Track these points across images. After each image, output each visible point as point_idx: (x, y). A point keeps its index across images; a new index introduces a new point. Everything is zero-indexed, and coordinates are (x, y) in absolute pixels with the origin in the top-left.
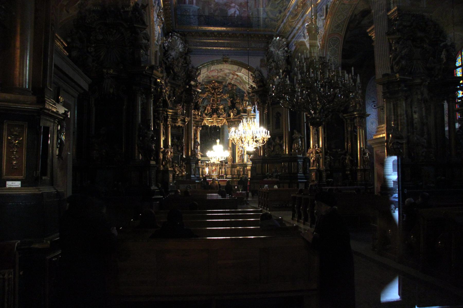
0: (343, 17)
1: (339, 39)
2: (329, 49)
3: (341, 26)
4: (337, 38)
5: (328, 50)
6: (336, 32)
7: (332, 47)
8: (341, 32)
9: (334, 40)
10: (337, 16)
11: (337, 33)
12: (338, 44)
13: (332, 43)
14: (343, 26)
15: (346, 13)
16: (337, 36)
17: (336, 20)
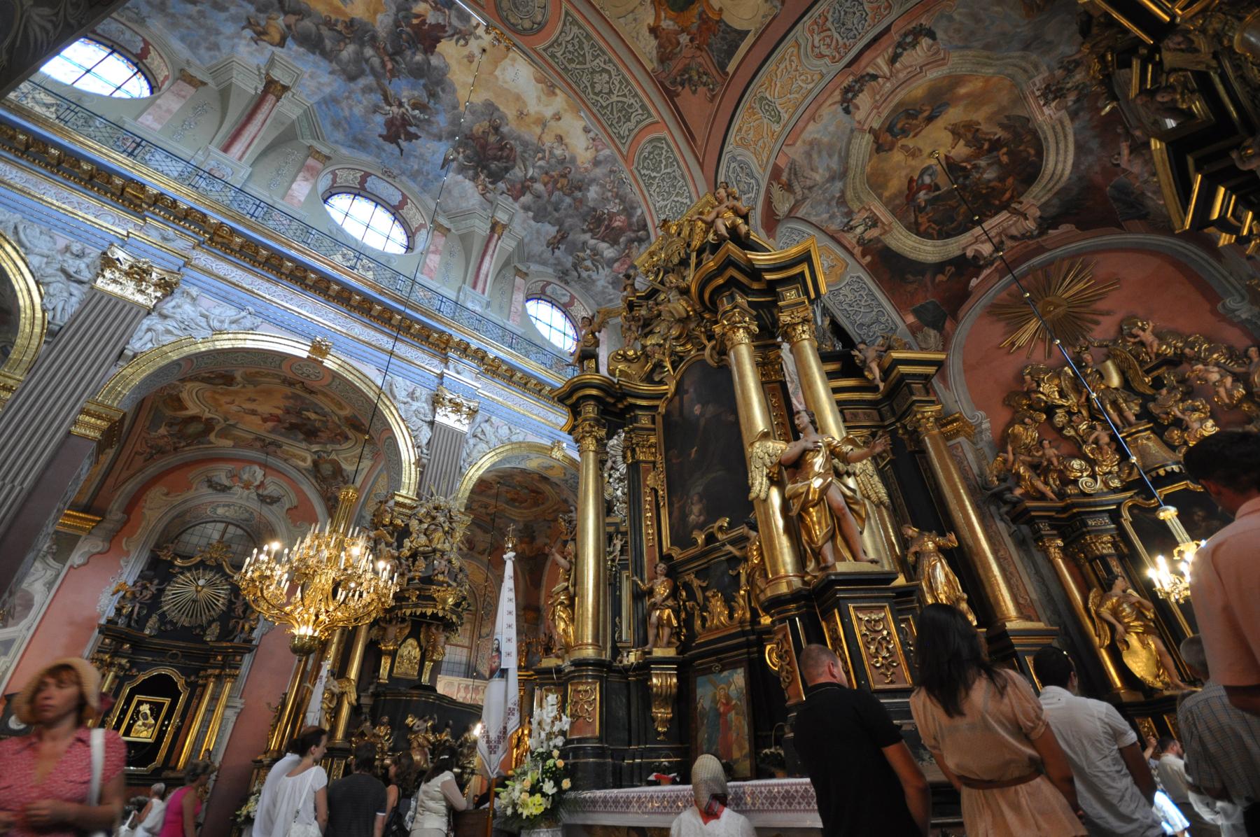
0: (606, 77)
1: (659, 139)
2: (652, 192)
3: (632, 101)
4: (651, 141)
5: (650, 195)
6: (636, 130)
7: (655, 177)
8: (650, 115)
9: (650, 153)
10: (592, 96)
11: (641, 131)
12: (667, 151)
13: (648, 169)
14: (636, 95)
15: (596, 57)
16: (649, 137)
17: (604, 104)
